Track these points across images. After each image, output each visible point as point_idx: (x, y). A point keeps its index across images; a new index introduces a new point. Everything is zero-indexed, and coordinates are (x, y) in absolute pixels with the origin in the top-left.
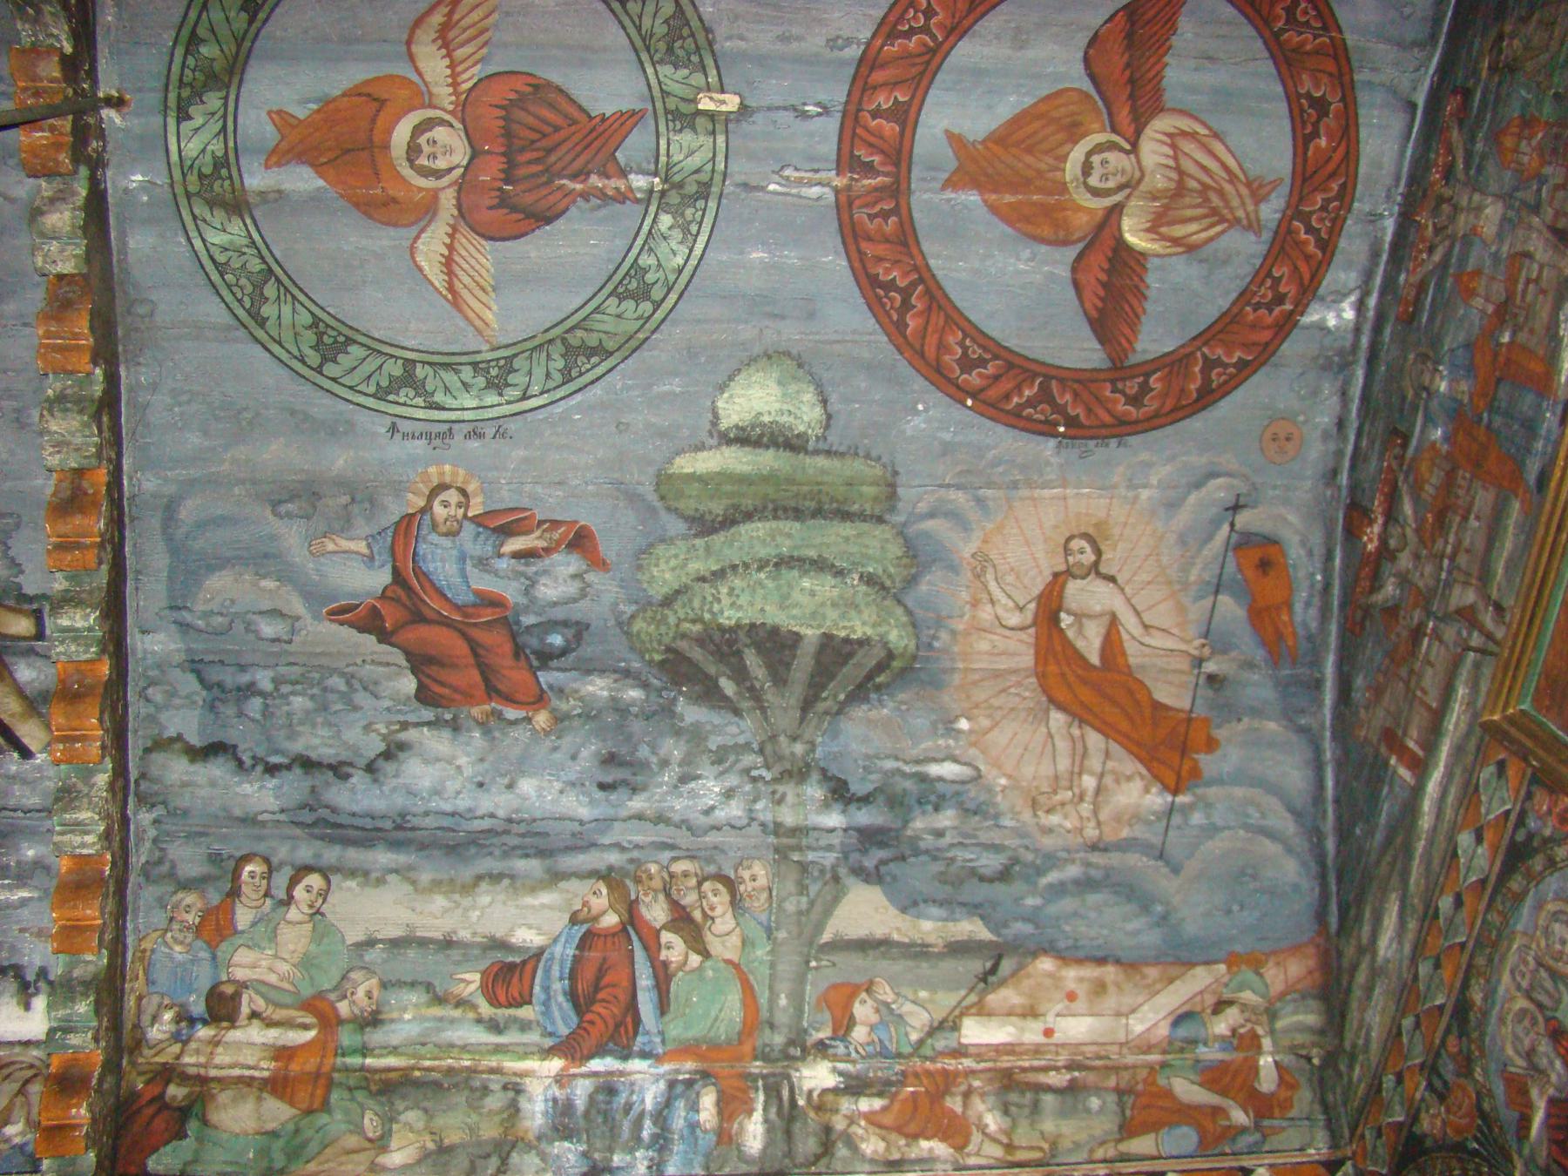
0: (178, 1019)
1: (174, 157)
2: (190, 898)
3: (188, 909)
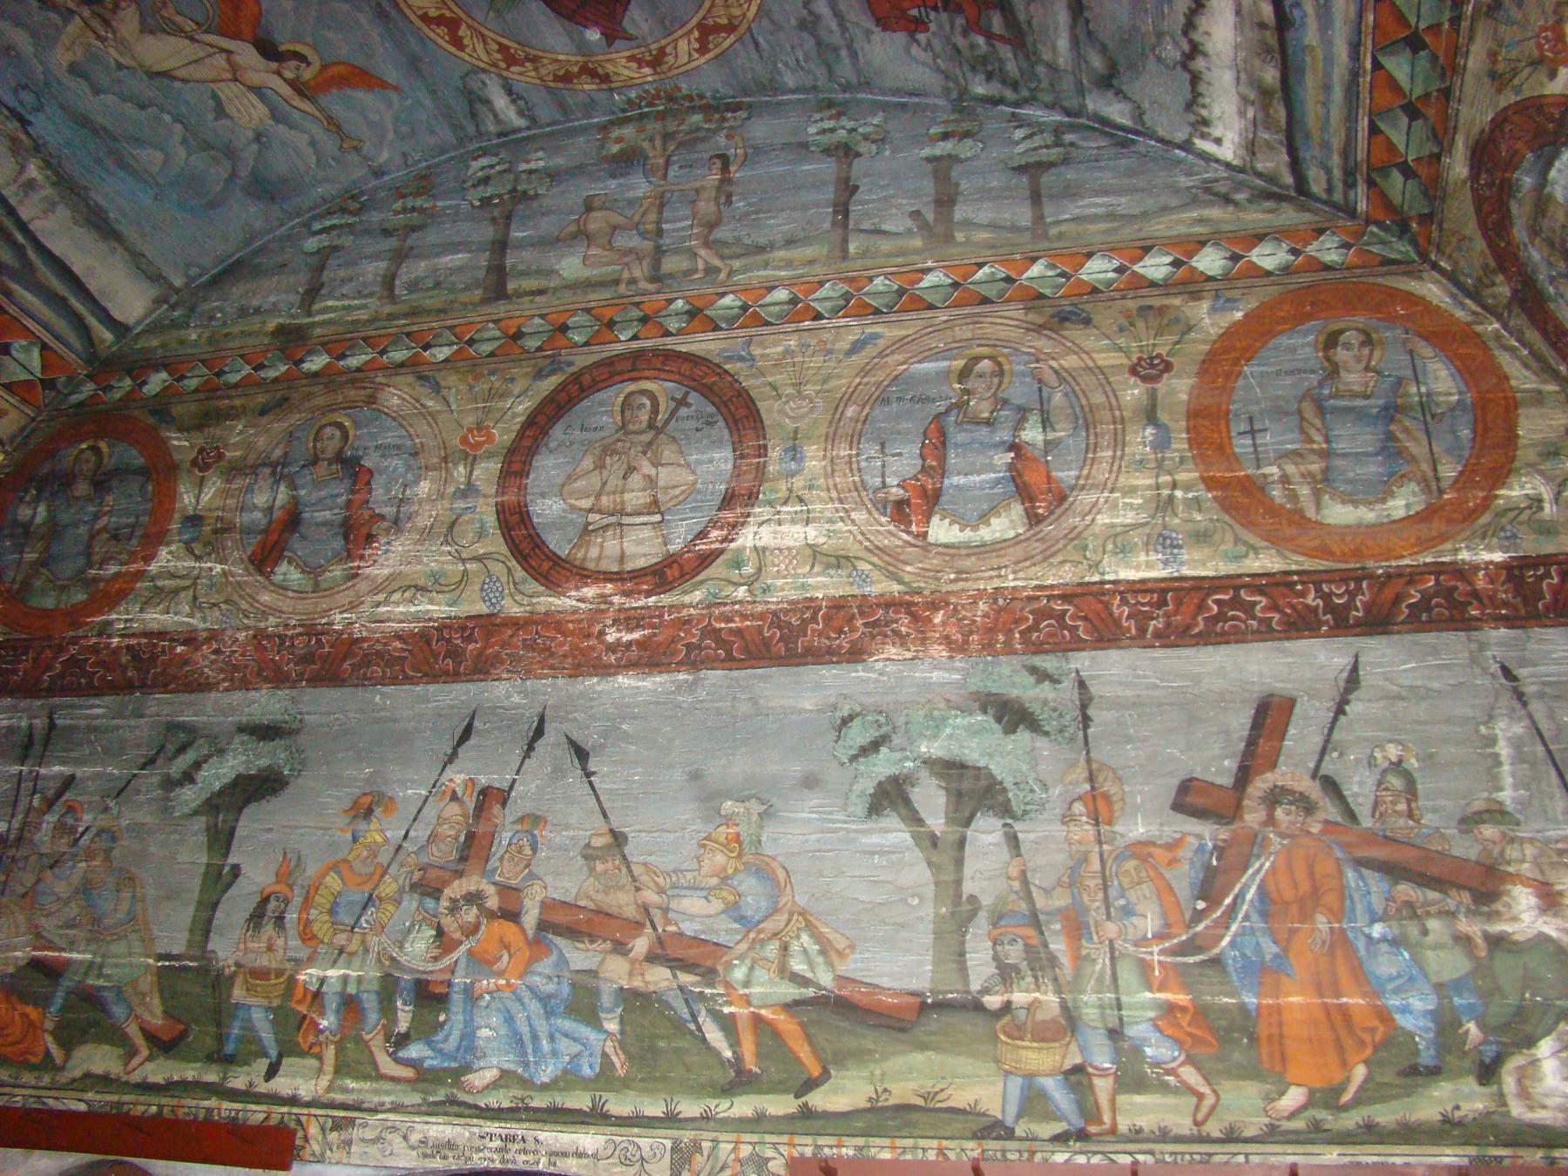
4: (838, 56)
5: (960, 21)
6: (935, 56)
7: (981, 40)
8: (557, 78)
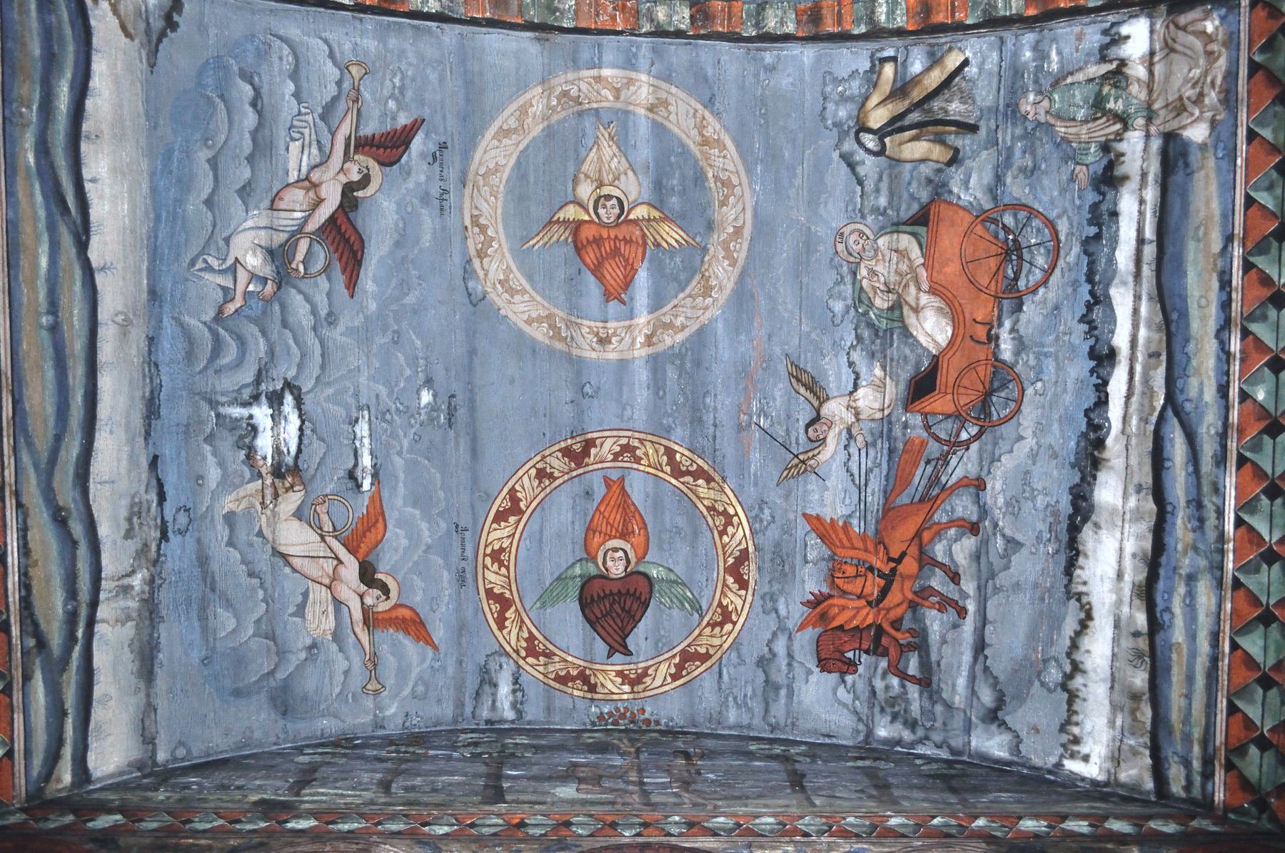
4: (777, 695)
5: (884, 664)
6: (856, 698)
7: (895, 681)
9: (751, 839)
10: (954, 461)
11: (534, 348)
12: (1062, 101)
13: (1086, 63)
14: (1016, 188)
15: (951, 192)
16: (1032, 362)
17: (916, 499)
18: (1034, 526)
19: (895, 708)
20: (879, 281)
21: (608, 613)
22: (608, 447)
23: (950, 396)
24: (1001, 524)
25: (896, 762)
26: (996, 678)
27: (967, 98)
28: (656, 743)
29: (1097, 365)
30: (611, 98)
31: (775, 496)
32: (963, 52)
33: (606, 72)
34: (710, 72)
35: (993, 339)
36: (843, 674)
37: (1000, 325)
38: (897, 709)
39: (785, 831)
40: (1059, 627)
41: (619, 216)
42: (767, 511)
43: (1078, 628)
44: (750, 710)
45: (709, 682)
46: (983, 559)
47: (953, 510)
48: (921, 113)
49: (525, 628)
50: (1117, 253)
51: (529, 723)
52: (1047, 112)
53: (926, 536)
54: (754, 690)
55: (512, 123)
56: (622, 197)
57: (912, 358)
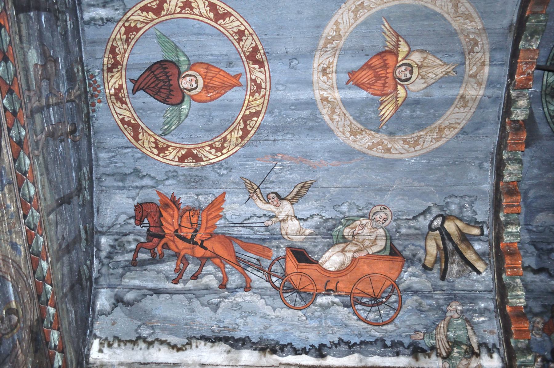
0: (543, 361)
1: (545, 83)
2: (538, 319)
3: (538, 323)
6: (122, 225)
7: (133, 246)
8: (113, 49)
9: (15, 183)
10: (259, 274)
11: (320, 27)
12: (458, 324)
13: (478, 336)
14: (410, 301)
15: (408, 267)
16: (316, 314)
17: (237, 254)
18: (227, 319)
19: (118, 247)
20: (359, 230)
21: (157, 79)
22: (259, 75)
23: (295, 271)
24: (226, 300)
25: (86, 251)
26: (141, 301)
27: (460, 274)
28: (79, 110)
29: (316, 349)
30: (471, 73)
31: (235, 176)
32: (485, 271)
33: (487, 69)
34: (481, 131)
35: (328, 292)
36: (135, 217)
37: (336, 296)
38: (118, 248)
39: (26, 203)
40: (170, 334)
41: (400, 79)
42: (225, 172)
43: (172, 344)
44: (108, 165)
45: (122, 141)
46: (205, 291)
47: (232, 274)
48: (452, 249)
49: (143, 25)
50: (377, 357)
51: (83, 30)
52: (451, 317)
53: (217, 261)
54: (120, 167)
55: (461, 9)
56: (411, 81)
57: (316, 250)
